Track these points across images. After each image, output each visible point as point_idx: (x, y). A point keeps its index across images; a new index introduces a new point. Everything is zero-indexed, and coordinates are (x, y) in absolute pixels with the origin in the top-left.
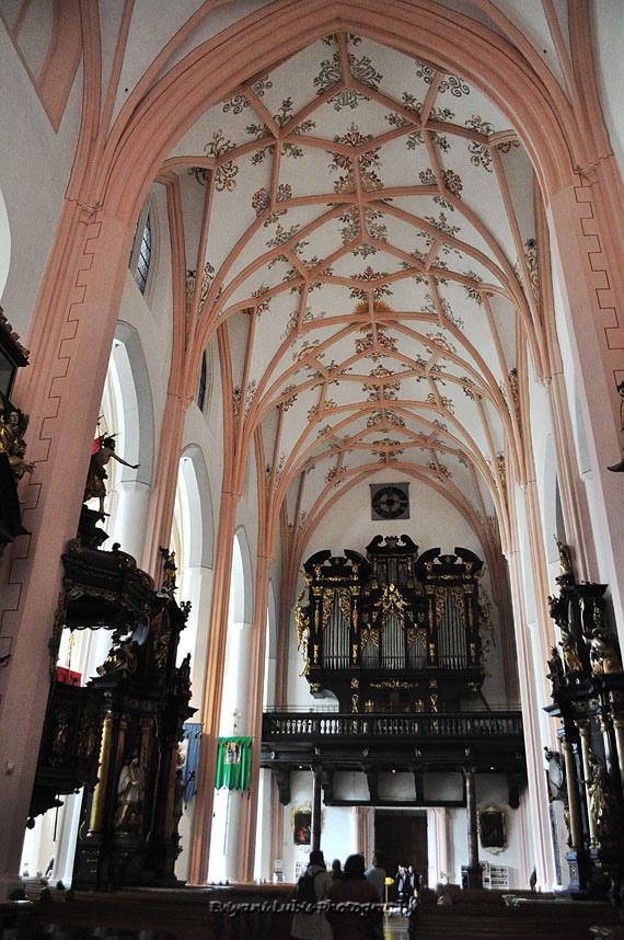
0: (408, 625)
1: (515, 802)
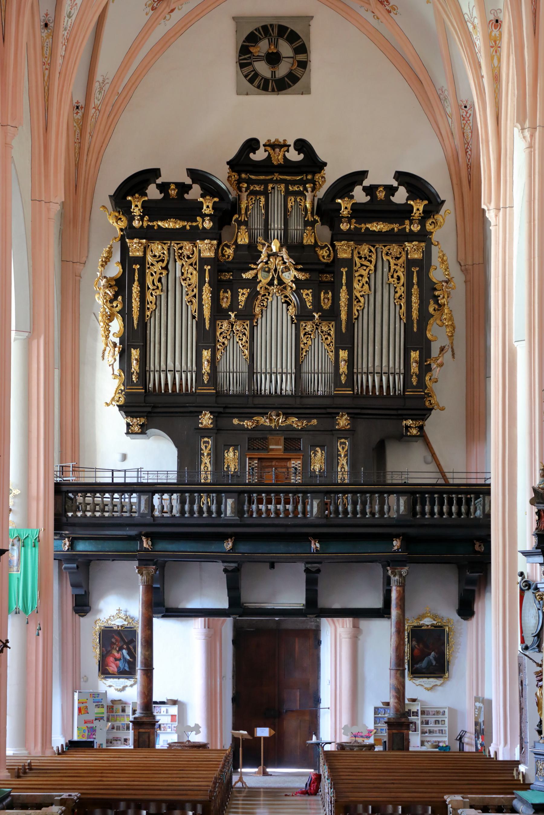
0: (303, 315)
1: (466, 610)
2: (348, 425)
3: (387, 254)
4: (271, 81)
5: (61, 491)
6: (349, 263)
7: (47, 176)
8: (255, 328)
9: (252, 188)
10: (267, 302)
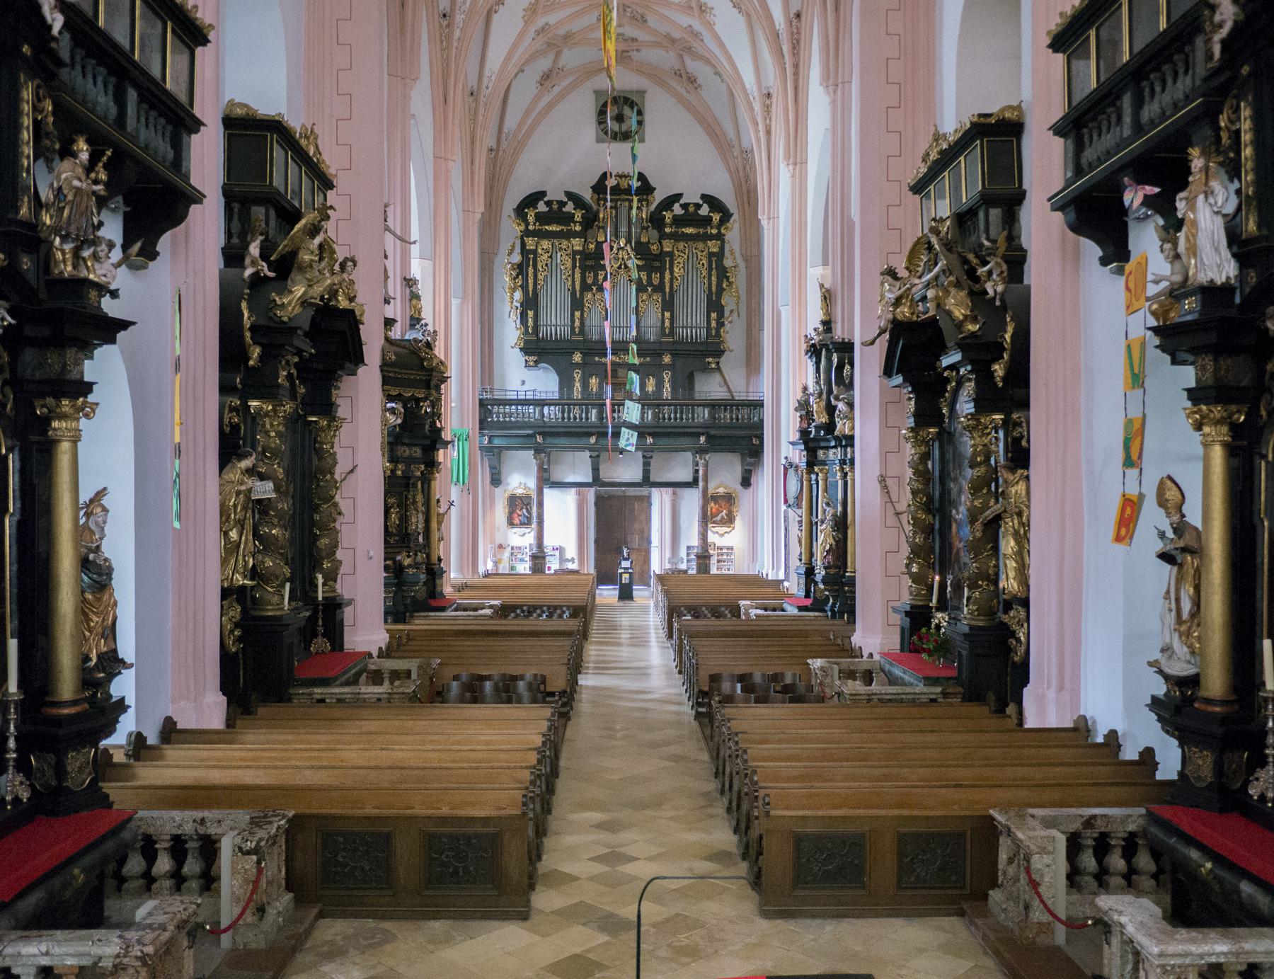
0: (641, 289)
1: (746, 482)
5: (482, 403)
6: (671, 254)
7: (473, 195)
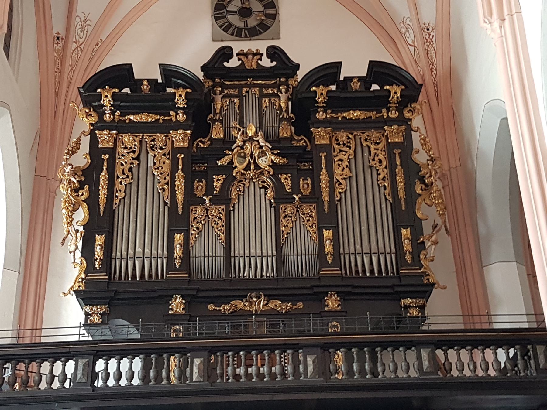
0: (281, 198)
2: (338, 306)
3: (366, 140)
4: (243, 30)
6: (328, 148)
8: (232, 212)
9: (226, 92)
10: (244, 187)
